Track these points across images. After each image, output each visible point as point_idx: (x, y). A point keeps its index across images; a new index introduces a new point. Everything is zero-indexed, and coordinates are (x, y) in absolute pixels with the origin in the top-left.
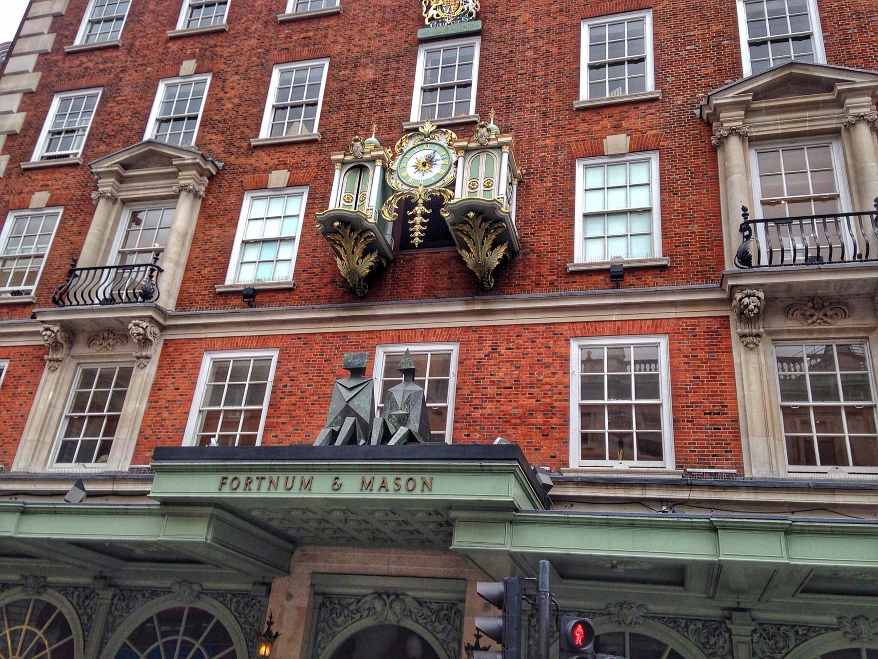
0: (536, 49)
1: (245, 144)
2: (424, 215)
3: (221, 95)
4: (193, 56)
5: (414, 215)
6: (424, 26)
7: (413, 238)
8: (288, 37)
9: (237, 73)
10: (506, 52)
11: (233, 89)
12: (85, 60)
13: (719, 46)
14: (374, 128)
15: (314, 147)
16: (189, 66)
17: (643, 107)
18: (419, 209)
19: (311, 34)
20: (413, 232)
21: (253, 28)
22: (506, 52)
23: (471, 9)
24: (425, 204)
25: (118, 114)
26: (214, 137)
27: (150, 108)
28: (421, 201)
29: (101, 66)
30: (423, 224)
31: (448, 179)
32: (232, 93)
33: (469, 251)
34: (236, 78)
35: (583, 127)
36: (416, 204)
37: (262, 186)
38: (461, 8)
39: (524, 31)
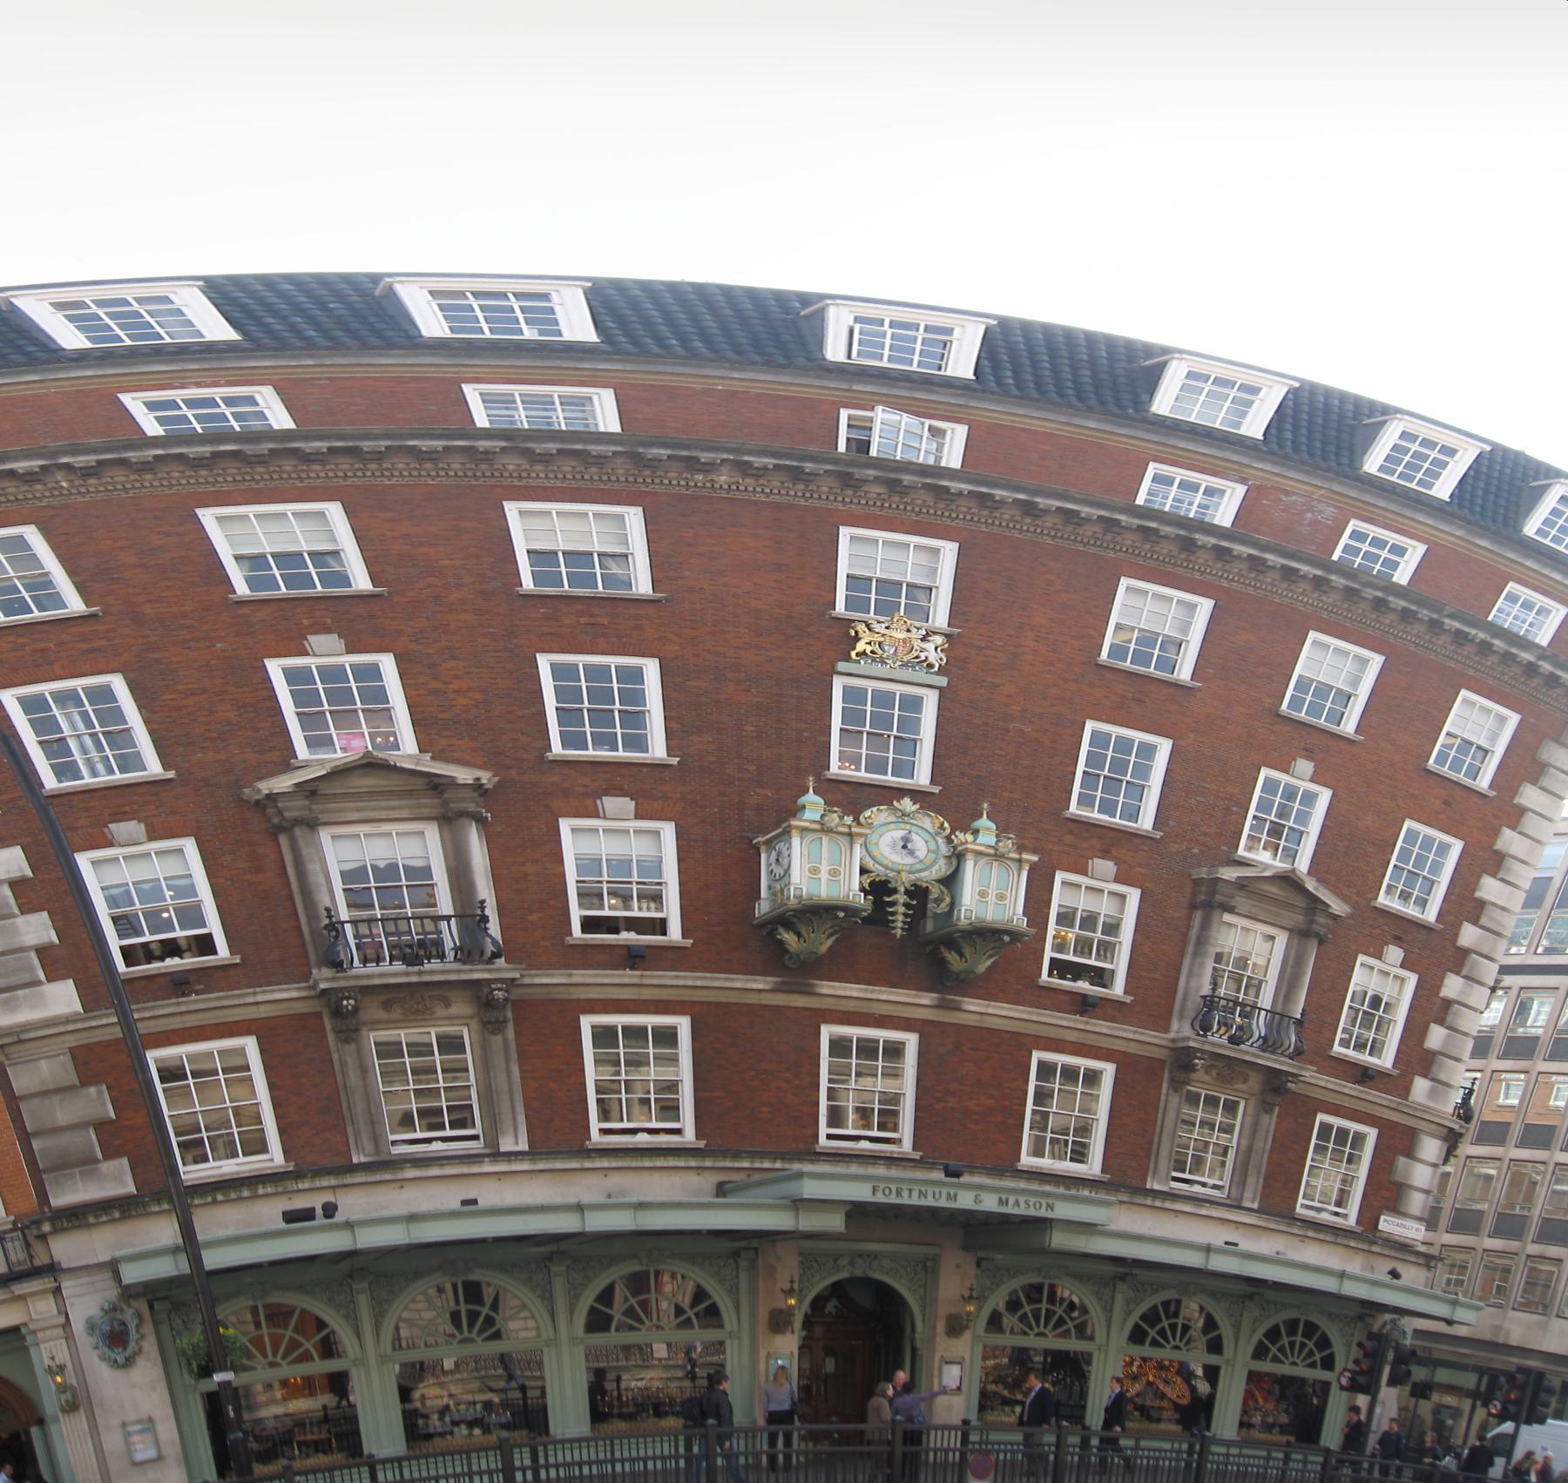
7: (894, 928)
20: (893, 922)
30: (905, 915)
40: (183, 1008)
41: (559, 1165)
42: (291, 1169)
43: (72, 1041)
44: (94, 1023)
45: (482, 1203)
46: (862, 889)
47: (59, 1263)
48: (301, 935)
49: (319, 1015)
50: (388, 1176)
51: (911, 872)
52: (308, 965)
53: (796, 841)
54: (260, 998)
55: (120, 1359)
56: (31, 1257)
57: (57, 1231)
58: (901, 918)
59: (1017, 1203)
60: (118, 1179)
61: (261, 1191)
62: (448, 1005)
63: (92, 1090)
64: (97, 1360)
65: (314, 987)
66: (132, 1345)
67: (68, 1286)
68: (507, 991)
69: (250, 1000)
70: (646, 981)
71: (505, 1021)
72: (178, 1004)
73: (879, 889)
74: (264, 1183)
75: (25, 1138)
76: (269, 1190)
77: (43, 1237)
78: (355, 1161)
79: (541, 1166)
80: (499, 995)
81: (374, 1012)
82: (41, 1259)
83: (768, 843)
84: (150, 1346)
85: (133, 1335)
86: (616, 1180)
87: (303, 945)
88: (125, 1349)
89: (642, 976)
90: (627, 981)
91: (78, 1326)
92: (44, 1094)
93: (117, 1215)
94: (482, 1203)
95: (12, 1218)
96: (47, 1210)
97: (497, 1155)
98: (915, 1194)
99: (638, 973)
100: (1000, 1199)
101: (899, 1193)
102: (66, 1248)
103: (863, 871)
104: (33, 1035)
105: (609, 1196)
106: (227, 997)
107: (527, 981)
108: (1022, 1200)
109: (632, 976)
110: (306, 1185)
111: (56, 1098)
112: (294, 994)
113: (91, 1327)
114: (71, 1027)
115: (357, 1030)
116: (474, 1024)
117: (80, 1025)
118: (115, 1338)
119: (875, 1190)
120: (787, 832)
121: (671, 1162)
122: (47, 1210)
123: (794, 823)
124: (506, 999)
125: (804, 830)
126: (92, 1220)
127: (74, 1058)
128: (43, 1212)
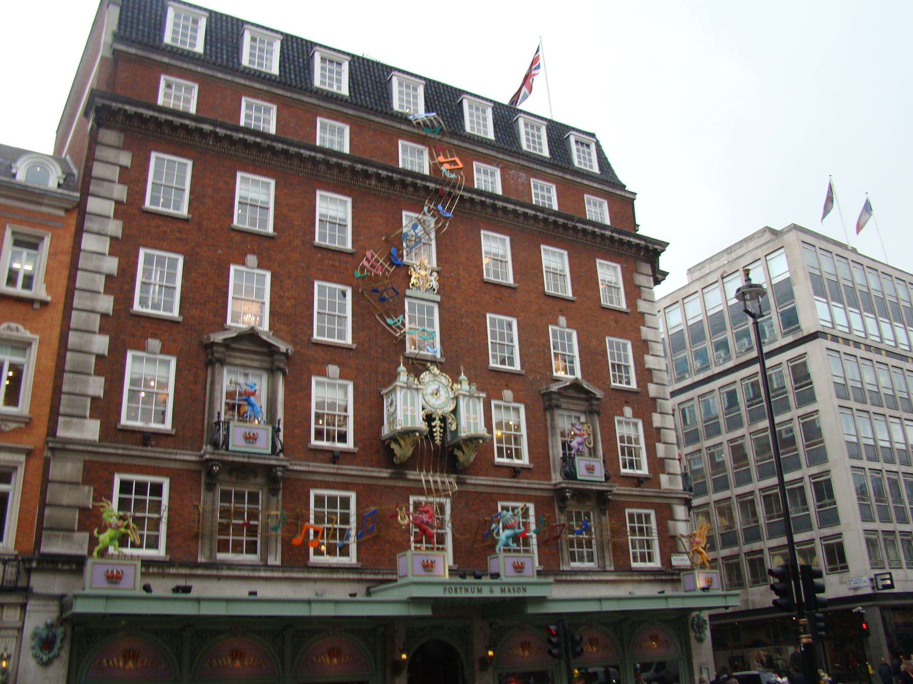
0: (467, 325)
1: (306, 339)
2: (441, 427)
3: (281, 293)
4: (253, 252)
5: (435, 427)
6: (409, 288)
8: (321, 260)
9: (289, 278)
10: (452, 320)
11: (288, 290)
12: (161, 223)
13: (544, 352)
14: (402, 361)
15: (351, 354)
16: (252, 259)
17: (517, 377)
18: (437, 422)
19: (337, 264)
21: (295, 243)
22: (452, 320)
23: (434, 287)
24: (440, 420)
25: (202, 285)
26: (282, 326)
27: (227, 287)
28: (437, 418)
29: (178, 235)
31: (452, 407)
32: (288, 294)
33: (463, 452)
34: (288, 281)
35: (493, 381)
36: (434, 419)
37: (323, 374)
38: (429, 283)
39: (460, 309)
40: (144, 454)
41: (295, 575)
42: (168, 559)
43: (87, 457)
44: (101, 450)
45: (259, 595)
46: (423, 419)
47: (32, 589)
48: (203, 425)
49: (200, 472)
50: (214, 572)
51: (441, 409)
52: (202, 443)
53: (398, 393)
54: (178, 457)
55: (45, 658)
56: (17, 580)
57: (39, 570)
58: (438, 433)
59: (509, 590)
60: (81, 546)
61: (151, 570)
62: (255, 477)
63: (86, 488)
64: (30, 654)
65: (202, 456)
66: (55, 651)
67: (32, 605)
68: (283, 472)
69: (173, 457)
70: (340, 472)
71: (279, 490)
72: (142, 451)
73: (429, 418)
74: (154, 567)
75: (43, 505)
76: (156, 570)
77: (29, 571)
78: (199, 560)
79: (287, 575)
80: (279, 474)
81: (224, 477)
82: (22, 583)
83: (387, 394)
84: (65, 654)
85: (58, 643)
86: (320, 586)
87: (203, 431)
88: (50, 651)
89: (338, 469)
90: (332, 471)
91: (28, 631)
92: (63, 482)
93: (74, 567)
94: (259, 595)
95: (16, 552)
96: (37, 552)
97: (267, 567)
98: (463, 590)
99: (336, 466)
100: (502, 589)
101: (456, 591)
102: (40, 583)
103: (423, 409)
104: (71, 447)
105: (317, 594)
106: (164, 453)
107: (291, 467)
108: (511, 588)
109: (334, 468)
110: (173, 571)
111: (67, 486)
112: (193, 458)
113: (35, 635)
114: (90, 449)
115: (215, 485)
116: (265, 490)
117: (95, 449)
118: (46, 643)
119: (445, 590)
120: (394, 389)
121: (346, 576)
122: (37, 552)
123: (398, 383)
124: (282, 477)
125: (402, 387)
126: (60, 566)
127: (85, 466)
128: (34, 553)
